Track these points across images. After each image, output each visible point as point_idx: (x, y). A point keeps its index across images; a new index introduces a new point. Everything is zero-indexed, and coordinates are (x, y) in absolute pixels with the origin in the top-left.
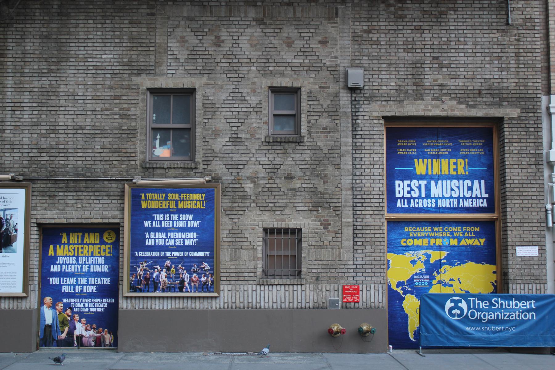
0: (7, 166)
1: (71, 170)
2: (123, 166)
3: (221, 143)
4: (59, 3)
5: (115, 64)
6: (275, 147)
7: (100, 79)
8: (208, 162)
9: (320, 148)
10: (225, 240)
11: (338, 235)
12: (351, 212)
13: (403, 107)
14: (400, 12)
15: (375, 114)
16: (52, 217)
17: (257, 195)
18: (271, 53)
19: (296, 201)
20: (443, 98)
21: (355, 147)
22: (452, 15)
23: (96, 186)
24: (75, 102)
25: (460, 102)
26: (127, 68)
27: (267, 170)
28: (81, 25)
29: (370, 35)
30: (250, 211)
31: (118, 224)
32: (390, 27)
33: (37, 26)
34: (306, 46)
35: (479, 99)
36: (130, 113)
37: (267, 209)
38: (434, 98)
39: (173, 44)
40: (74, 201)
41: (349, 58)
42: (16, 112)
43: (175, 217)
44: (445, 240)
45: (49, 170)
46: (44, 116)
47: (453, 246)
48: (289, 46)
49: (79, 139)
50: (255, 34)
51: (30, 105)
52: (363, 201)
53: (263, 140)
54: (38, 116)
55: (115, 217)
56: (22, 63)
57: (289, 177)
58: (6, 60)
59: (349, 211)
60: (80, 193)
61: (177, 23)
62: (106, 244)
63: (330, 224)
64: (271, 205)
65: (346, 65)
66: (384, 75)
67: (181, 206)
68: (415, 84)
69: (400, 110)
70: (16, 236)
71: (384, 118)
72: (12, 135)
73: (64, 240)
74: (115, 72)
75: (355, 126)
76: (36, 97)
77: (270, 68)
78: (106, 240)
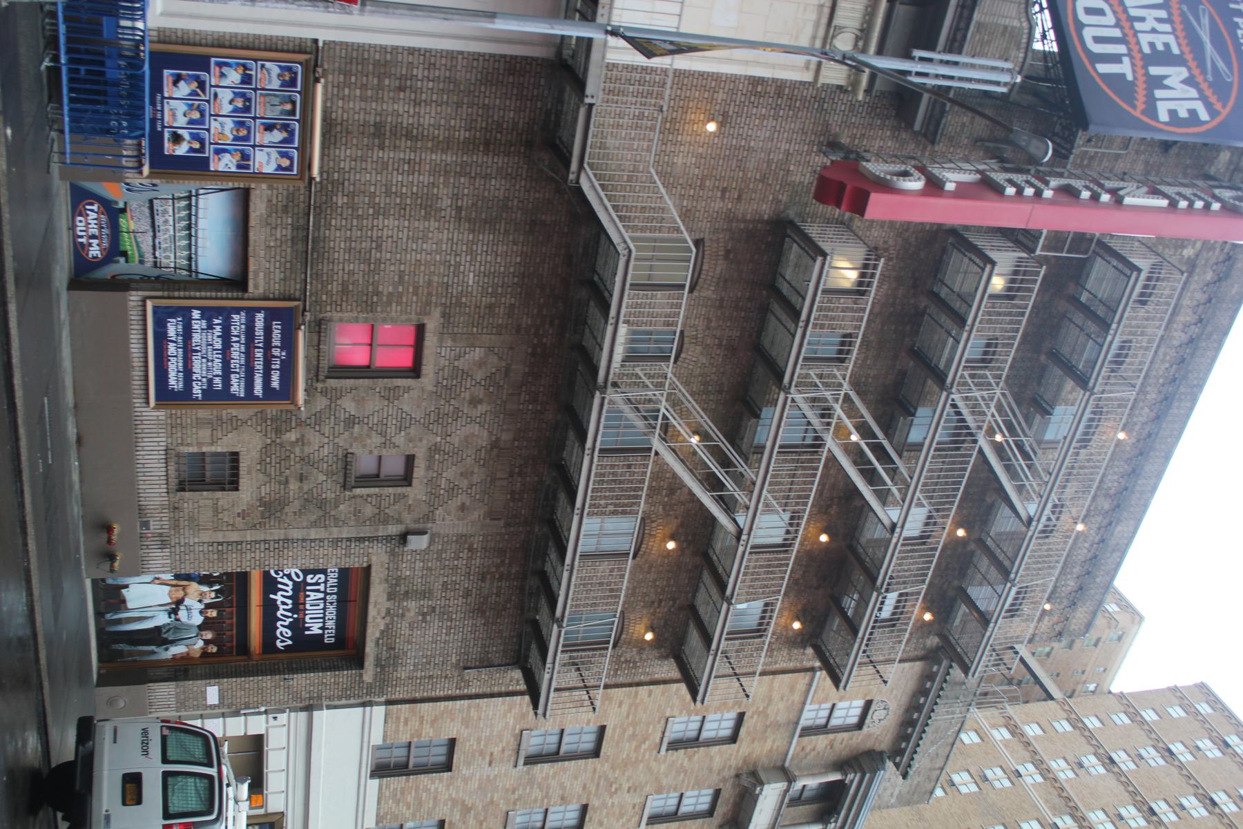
2: (324, 297)
3: (349, 405)
8: (324, 392)
9: (337, 507)
15: (374, 559)
17: (281, 445)
21: (336, 542)
24: (415, 240)
25: (382, 632)
26: (454, 300)
31: (245, 289)
38: (388, 611)
39: (478, 353)
40: (279, 236)
46: (398, 200)
48: (462, 474)
55: (256, 287)
57: (301, 478)
59: (260, 535)
60: (289, 243)
68: (407, 592)
69: (378, 581)
71: (369, 567)
75: (361, 540)
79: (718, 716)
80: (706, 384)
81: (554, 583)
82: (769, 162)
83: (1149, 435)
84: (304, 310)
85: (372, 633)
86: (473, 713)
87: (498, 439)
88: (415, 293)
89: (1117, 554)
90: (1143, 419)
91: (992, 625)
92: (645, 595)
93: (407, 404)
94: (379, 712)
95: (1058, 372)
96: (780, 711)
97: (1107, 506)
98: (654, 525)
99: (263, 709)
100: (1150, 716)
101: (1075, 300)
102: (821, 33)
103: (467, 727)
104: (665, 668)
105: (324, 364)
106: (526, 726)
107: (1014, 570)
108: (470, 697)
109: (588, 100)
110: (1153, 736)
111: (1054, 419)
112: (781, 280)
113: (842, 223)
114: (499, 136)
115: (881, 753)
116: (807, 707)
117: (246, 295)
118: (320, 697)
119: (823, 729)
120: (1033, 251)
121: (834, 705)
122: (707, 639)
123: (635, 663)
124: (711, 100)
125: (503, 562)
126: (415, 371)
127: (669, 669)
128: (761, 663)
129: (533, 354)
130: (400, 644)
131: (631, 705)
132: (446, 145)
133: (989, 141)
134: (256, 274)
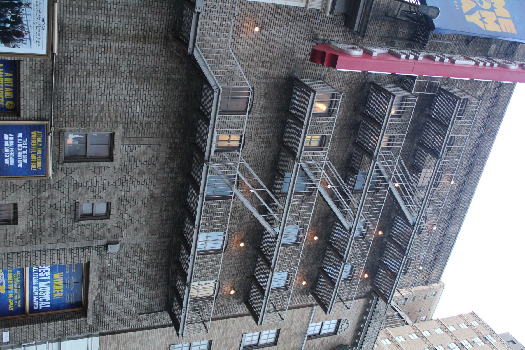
0: (64, 41)
1: (60, 85)
2: (61, 119)
3: (76, 177)
4: (176, 79)
5: (132, 114)
6: (72, 207)
7: (123, 104)
8: (63, 170)
10: (9, 182)
11: (14, 245)
12: (29, 250)
13: (95, 271)
14: (151, 265)
15: (91, 258)
16: (25, 71)
17: (40, 199)
18: (132, 202)
19: (36, 221)
20: (99, 290)
21: (71, 250)
22: (147, 289)
23: (48, 101)
25: (96, 297)
26: (129, 121)
27: (57, 204)
28: (160, 93)
29: (139, 252)
30: (29, 195)
31: (19, 115)
32: (143, 261)
33: (163, 65)
34: (135, 221)
35: (98, 306)
36: (98, 123)
37: (31, 205)
38: (99, 285)
39: (142, 148)
40: (36, 86)
41: (126, 243)
42: (103, 49)
43: (25, 152)
44: (12, 292)
45: (60, 71)
46: (99, 67)
47: (8, 296)
48: (135, 212)
49: (82, 91)
50: (144, 194)
51: (108, 58)
52: (37, 255)
53: (77, 201)
54: (99, 64)
55: (25, 114)
56: (138, 54)
57: (52, 216)
58: (141, 43)
59: (30, 248)
60: (42, 90)
61: (156, 150)
62: (5, 102)
63: (21, 239)
64: (34, 207)
65: (122, 241)
66: (115, 260)
67: (33, 155)
68: (109, 276)
69: (93, 270)
70: (9, 46)
71: (89, 263)
72: (87, 45)
73: (7, 74)
74: (127, 114)
75: (84, 248)
76: (113, 63)
77: (122, 203)
78: (7, 103)
79: (267, 332)
80: (256, 161)
81: (184, 266)
82: (285, 48)
83: (464, 182)
84: (51, 126)
85: (91, 298)
86: (145, 338)
87: (154, 193)
88: (109, 116)
90: (462, 175)
91: (398, 277)
92: (229, 271)
93: (106, 175)
94: (96, 339)
95: (424, 152)
96: (297, 327)
97: (446, 218)
98: (233, 235)
99: (34, 342)
100: (451, 329)
101: (430, 117)
103: (142, 345)
105: (62, 155)
106: (172, 343)
107: (407, 249)
108: (143, 329)
109: (197, 10)
110: (454, 338)
111: (422, 175)
112: (292, 107)
113: (320, 79)
114: (150, 34)
115: (346, 346)
116: (311, 325)
117: (20, 118)
118: (64, 334)
119: (318, 335)
120: (410, 91)
121: (323, 323)
122: (262, 292)
123: (225, 306)
124: (256, 17)
125: (157, 257)
126: (110, 158)
127: (243, 309)
128: (289, 302)
129: (170, 148)
130: (106, 303)
131: (224, 329)
132: (123, 38)
133: (388, 38)
134: (25, 107)
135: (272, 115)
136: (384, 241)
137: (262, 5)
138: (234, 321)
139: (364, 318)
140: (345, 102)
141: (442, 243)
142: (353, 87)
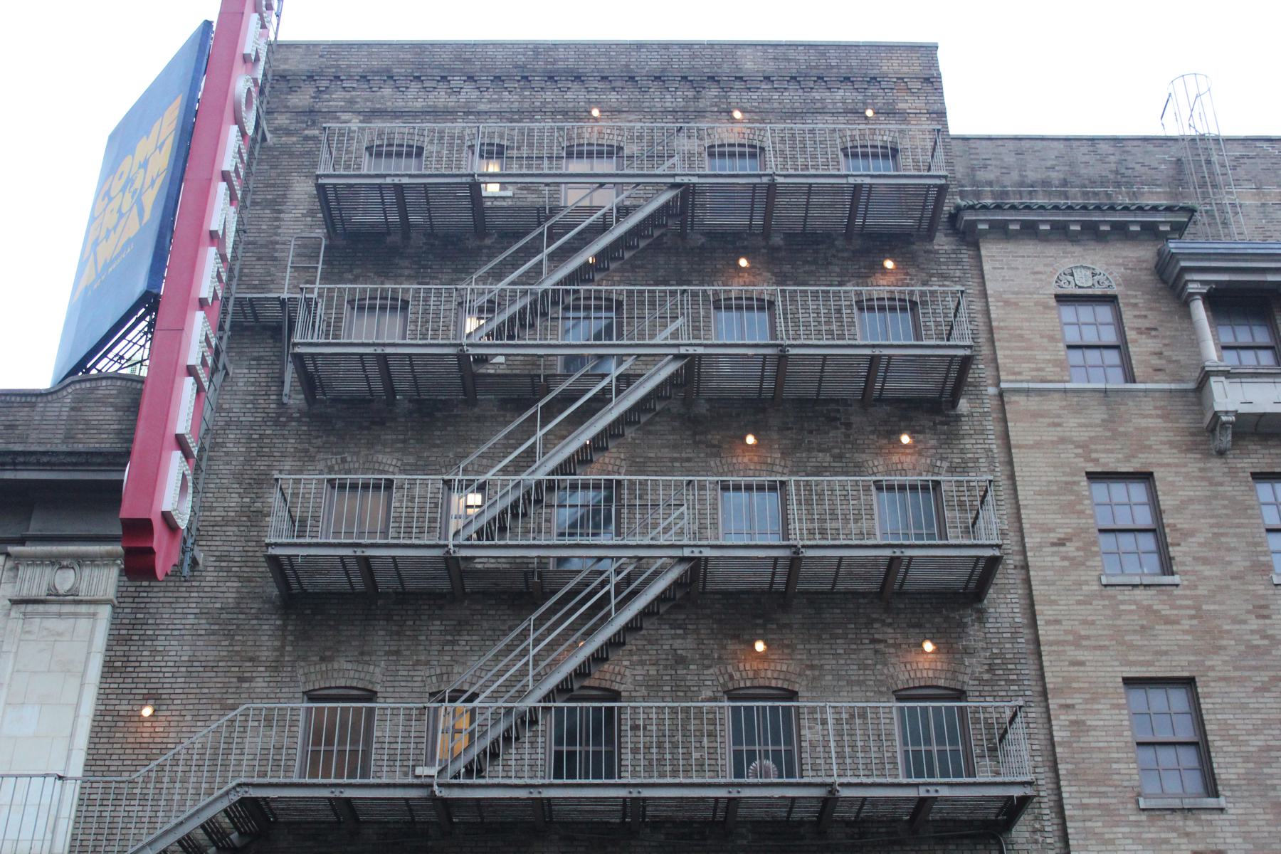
83: (604, 78)
89: (791, 53)
90: (583, 92)
97: (714, 92)
98: (737, 675)
102: (54, 608)
104: (1003, 609)
135: (382, 633)
136: (781, 243)
137: (103, 708)
138: (1048, 623)
139: (1047, 227)
140: (357, 454)
141: (794, 78)
142: (319, 442)
